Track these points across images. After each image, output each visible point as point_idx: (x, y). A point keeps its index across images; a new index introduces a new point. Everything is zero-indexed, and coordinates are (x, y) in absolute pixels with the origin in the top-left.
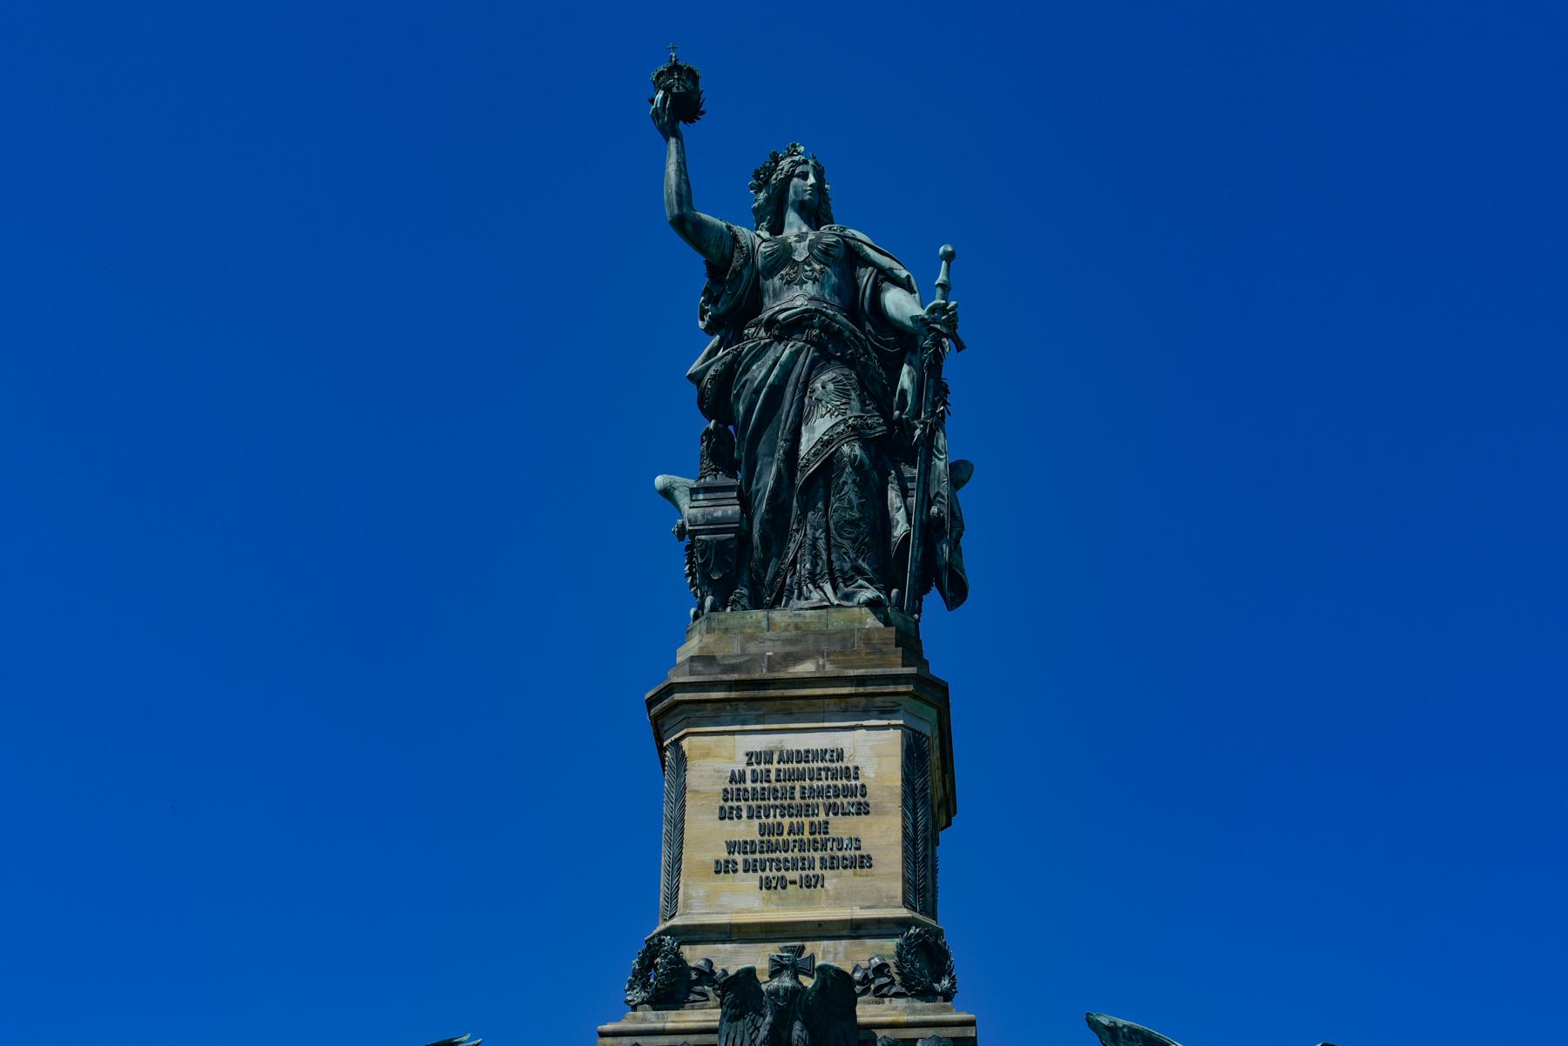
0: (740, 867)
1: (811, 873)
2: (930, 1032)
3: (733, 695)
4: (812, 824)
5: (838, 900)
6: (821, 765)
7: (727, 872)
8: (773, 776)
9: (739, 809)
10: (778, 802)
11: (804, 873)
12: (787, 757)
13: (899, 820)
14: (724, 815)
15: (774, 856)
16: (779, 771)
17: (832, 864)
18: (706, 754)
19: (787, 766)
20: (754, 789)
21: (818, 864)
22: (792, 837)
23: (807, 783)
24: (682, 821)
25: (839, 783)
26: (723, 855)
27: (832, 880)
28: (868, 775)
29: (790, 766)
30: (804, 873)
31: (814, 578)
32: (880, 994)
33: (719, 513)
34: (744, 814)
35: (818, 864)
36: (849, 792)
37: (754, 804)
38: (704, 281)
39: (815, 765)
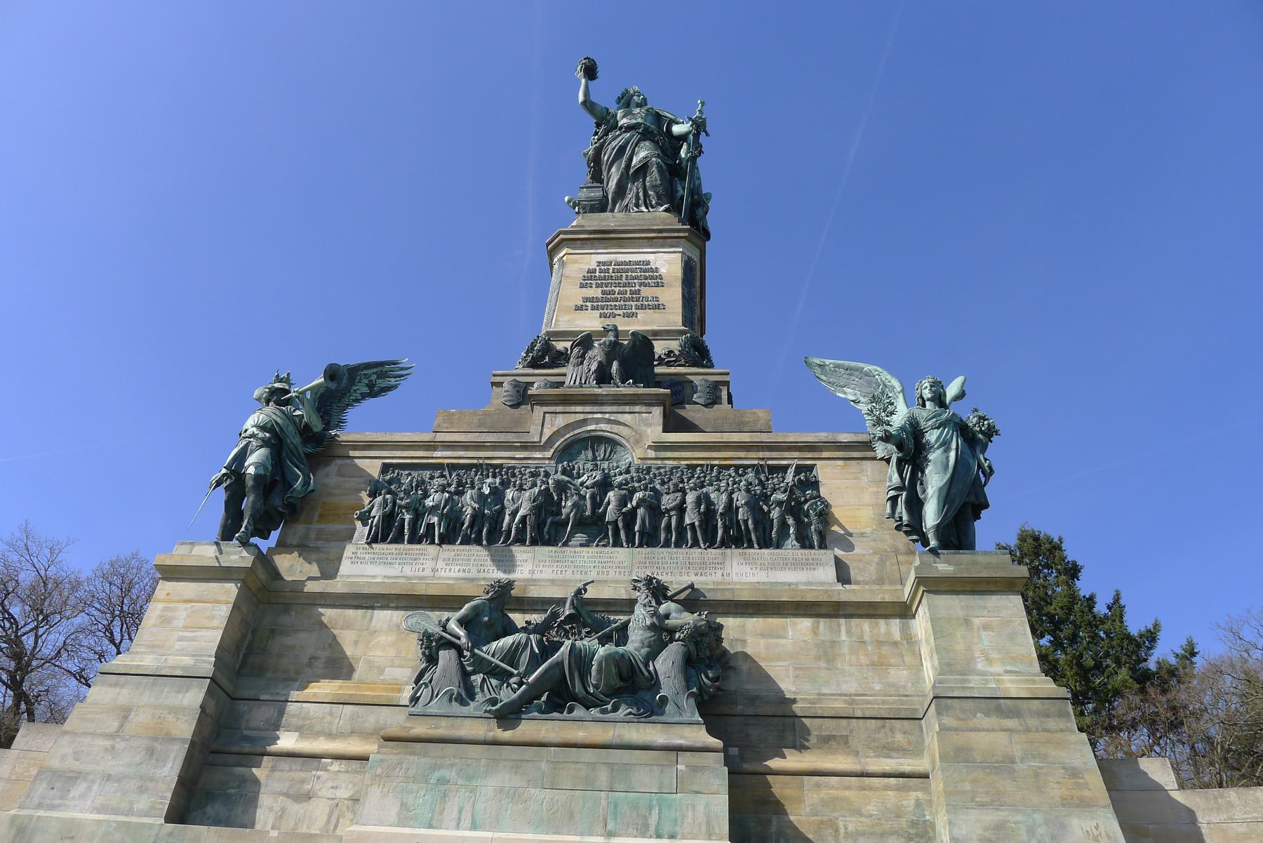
5: (644, 323)
12: (617, 264)
13: (680, 290)
14: (582, 286)
17: (642, 307)
27: (641, 315)
28: (663, 271)
31: (637, 205)
32: (669, 364)
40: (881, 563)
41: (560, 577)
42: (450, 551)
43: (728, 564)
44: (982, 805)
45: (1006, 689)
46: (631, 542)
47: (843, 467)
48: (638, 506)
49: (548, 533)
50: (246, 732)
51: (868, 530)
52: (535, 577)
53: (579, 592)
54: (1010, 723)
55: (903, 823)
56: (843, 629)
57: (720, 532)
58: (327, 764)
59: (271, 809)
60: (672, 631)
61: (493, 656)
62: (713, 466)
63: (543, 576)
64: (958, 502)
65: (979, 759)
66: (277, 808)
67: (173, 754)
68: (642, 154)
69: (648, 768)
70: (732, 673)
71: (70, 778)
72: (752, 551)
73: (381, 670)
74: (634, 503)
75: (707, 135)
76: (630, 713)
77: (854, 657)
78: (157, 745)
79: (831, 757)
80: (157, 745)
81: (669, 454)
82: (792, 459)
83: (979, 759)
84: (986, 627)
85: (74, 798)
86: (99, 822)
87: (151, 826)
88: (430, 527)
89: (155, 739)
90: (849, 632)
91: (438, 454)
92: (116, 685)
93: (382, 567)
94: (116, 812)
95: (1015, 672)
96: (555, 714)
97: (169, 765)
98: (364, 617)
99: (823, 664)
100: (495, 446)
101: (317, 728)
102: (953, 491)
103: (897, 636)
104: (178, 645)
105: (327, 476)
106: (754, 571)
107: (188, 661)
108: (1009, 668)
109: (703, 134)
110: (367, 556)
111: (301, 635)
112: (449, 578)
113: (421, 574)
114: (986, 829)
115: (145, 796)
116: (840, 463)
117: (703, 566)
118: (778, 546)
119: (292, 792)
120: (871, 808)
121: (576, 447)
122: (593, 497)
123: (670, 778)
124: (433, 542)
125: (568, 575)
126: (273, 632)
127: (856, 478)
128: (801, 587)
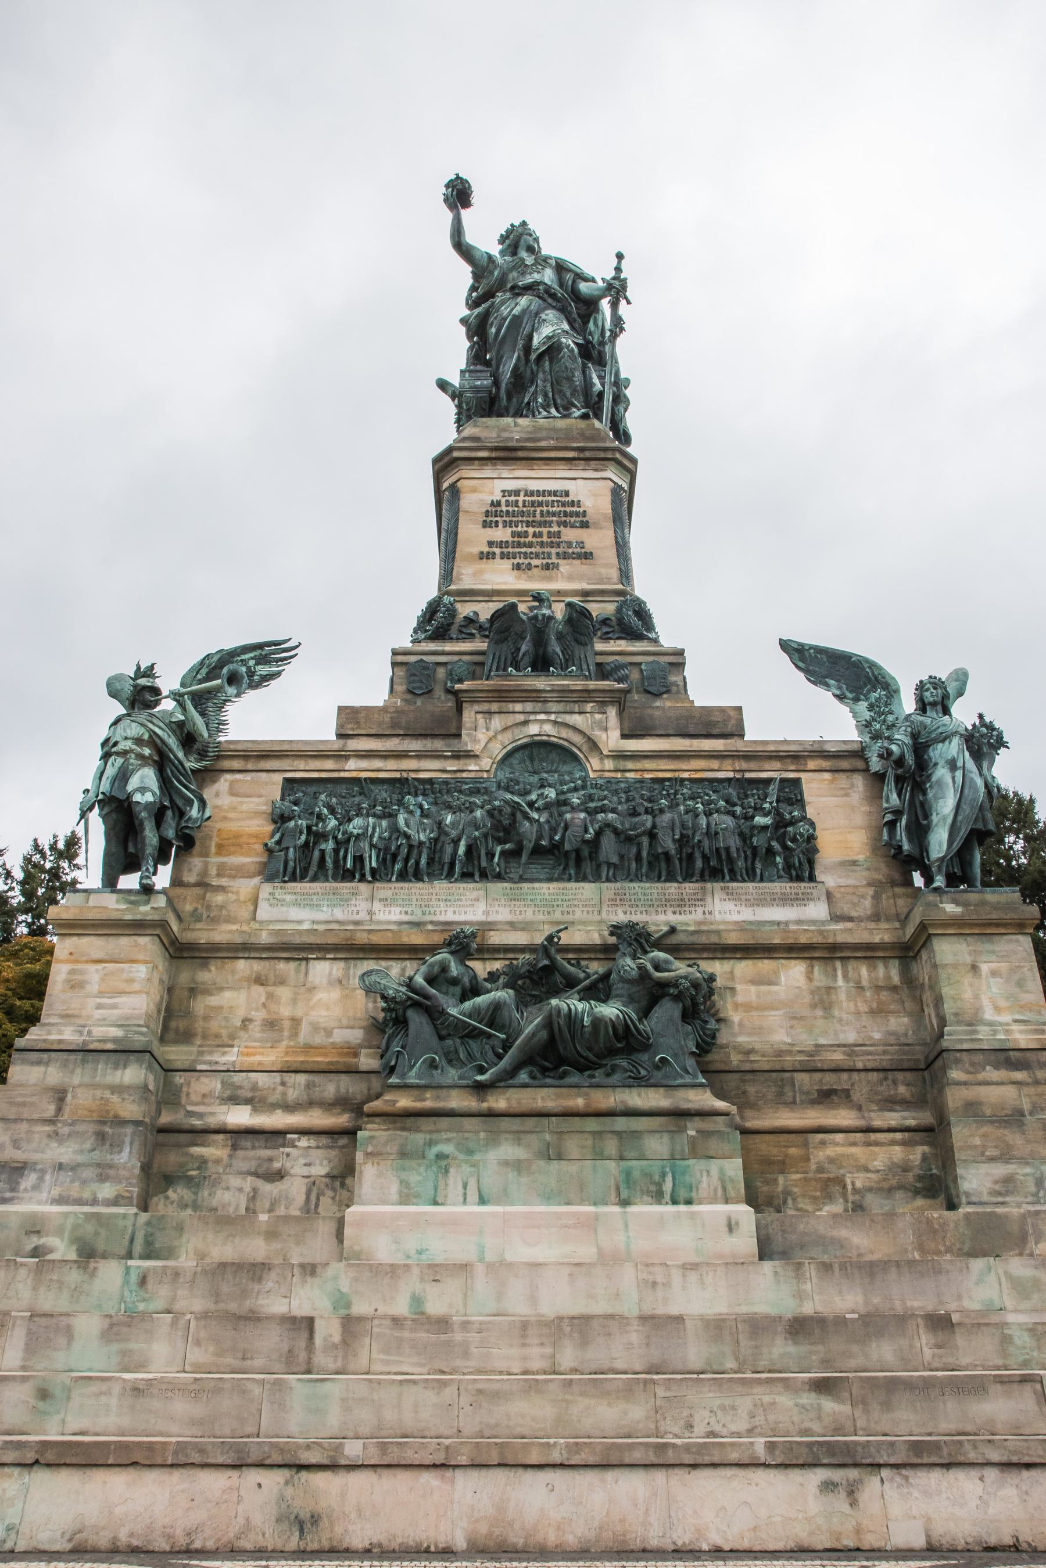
0: (498, 556)
1: (550, 561)
2: (651, 658)
3: (494, 455)
4: (549, 532)
5: (570, 578)
6: (555, 499)
7: (488, 558)
8: (520, 504)
9: (497, 522)
10: (524, 519)
11: (545, 561)
12: (532, 494)
13: (611, 533)
14: (486, 525)
15: (523, 550)
16: (524, 501)
17: (565, 556)
18: (474, 490)
19: (530, 499)
20: (508, 511)
21: (554, 556)
22: (535, 540)
23: (545, 509)
24: (457, 528)
25: (568, 509)
26: (486, 549)
27: (565, 567)
28: (588, 503)
29: (533, 498)
30: (545, 561)
32: (605, 638)
33: (479, 383)
34: (500, 525)
35: (554, 556)
36: (577, 514)
37: (507, 519)
38: (471, 281)
39: (550, 499)
40: (876, 897)
41: (520, 918)
42: (385, 890)
43: (709, 899)
44: (992, 1159)
45: (1015, 1040)
46: (597, 878)
47: (832, 781)
48: (598, 834)
49: (498, 865)
50: (190, 1108)
51: (861, 857)
52: (490, 919)
53: (550, 938)
54: (1019, 1075)
55: (910, 1177)
56: (839, 973)
57: (699, 863)
58: (293, 1140)
59: (241, 1190)
60: (663, 986)
61: (470, 1017)
62: (683, 780)
63: (499, 918)
64: (963, 833)
65: (988, 1112)
66: (247, 1188)
67: (128, 1140)
68: (546, 331)
69: (657, 1136)
70: (722, 1026)
71: (17, 1168)
72: (735, 885)
73: (329, 1033)
74: (597, 826)
75: (629, 303)
76: (630, 1077)
77: (852, 1004)
78: (107, 1129)
79: (834, 1112)
80: (107, 1129)
81: (630, 765)
82: (771, 772)
83: (988, 1112)
84: (994, 974)
85: (26, 1190)
86: (66, 1215)
87: (125, 1216)
88: (359, 859)
89: (102, 1122)
90: (845, 976)
91: (352, 764)
92: (39, 1063)
93: (307, 909)
94: (79, 1202)
95: (1024, 1021)
96: (548, 1081)
97: (127, 1150)
98: (298, 971)
99: (819, 1013)
100: (420, 756)
101: (272, 1099)
102: (960, 818)
103: (896, 979)
104: (98, 1014)
105: (217, 795)
106: (738, 908)
107: (117, 1032)
108: (1018, 1017)
109: (623, 302)
110: (288, 897)
111: (227, 994)
112: (389, 923)
113: (356, 918)
114: (996, 1182)
115: (107, 1184)
116: (827, 776)
117: (680, 904)
118: (762, 880)
119: (261, 1171)
120: (878, 1164)
121: (518, 755)
122: (548, 822)
123: (682, 1142)
124: (363, 879)
125: (529, 915)
126: (193, 991)
127: (847, 795)
128: (793, 927)
